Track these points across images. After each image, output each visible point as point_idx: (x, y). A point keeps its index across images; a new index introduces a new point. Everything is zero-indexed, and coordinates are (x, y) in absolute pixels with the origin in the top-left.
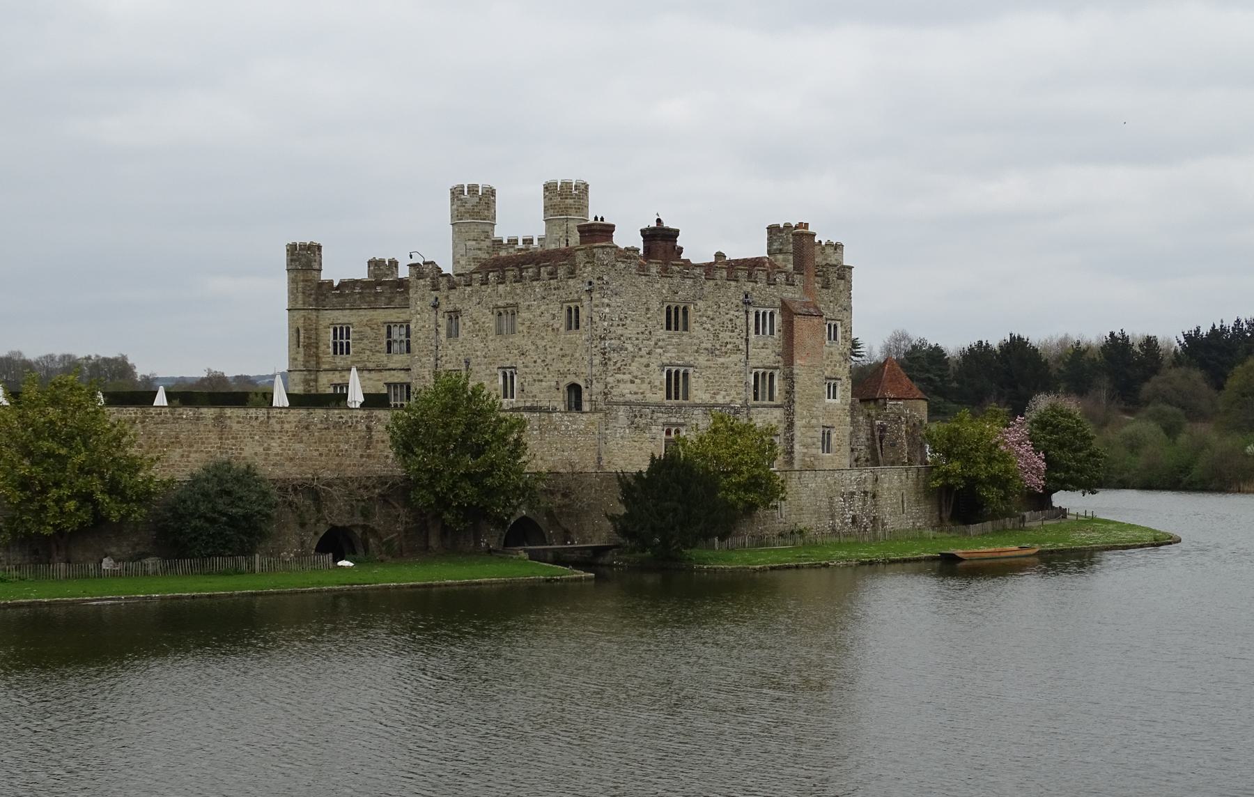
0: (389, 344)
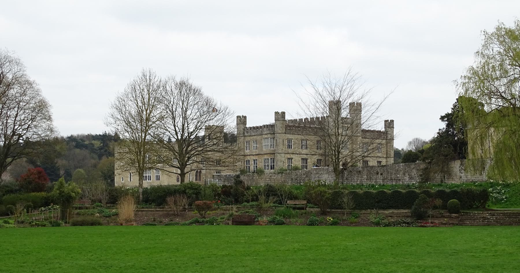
0: (302, 146)
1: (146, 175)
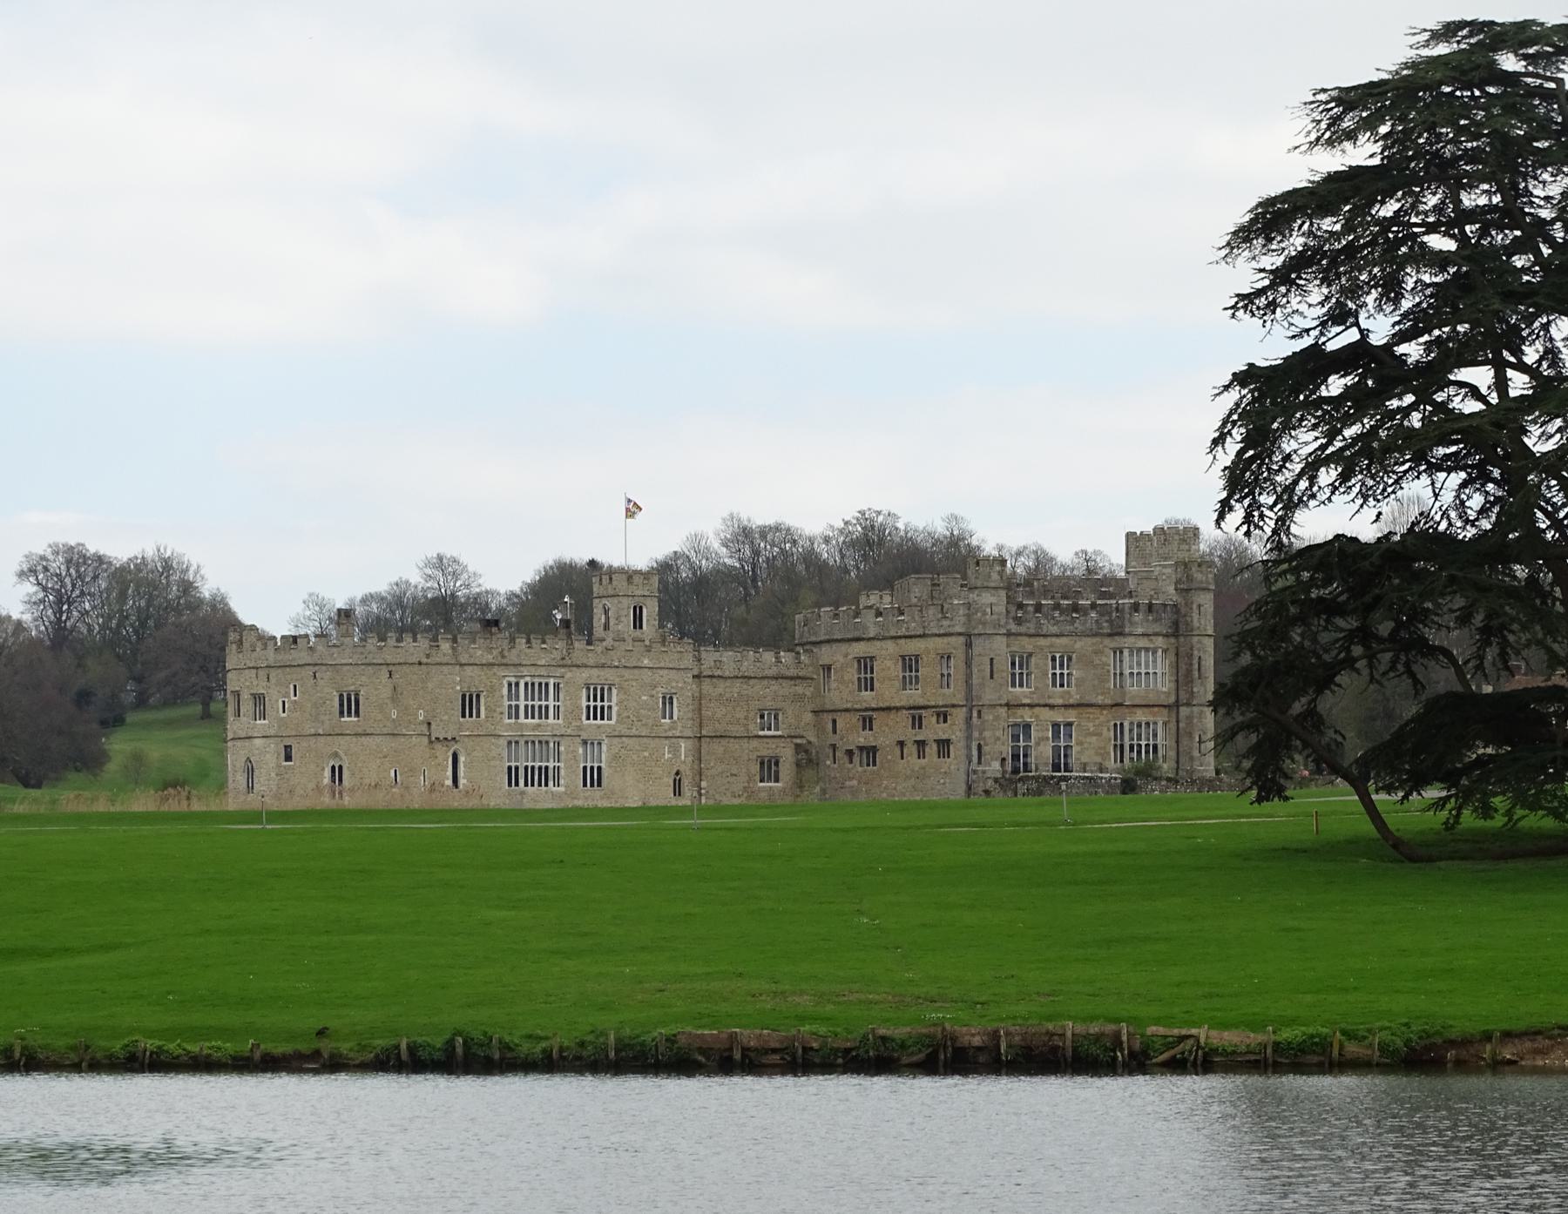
1: (544, 764)
